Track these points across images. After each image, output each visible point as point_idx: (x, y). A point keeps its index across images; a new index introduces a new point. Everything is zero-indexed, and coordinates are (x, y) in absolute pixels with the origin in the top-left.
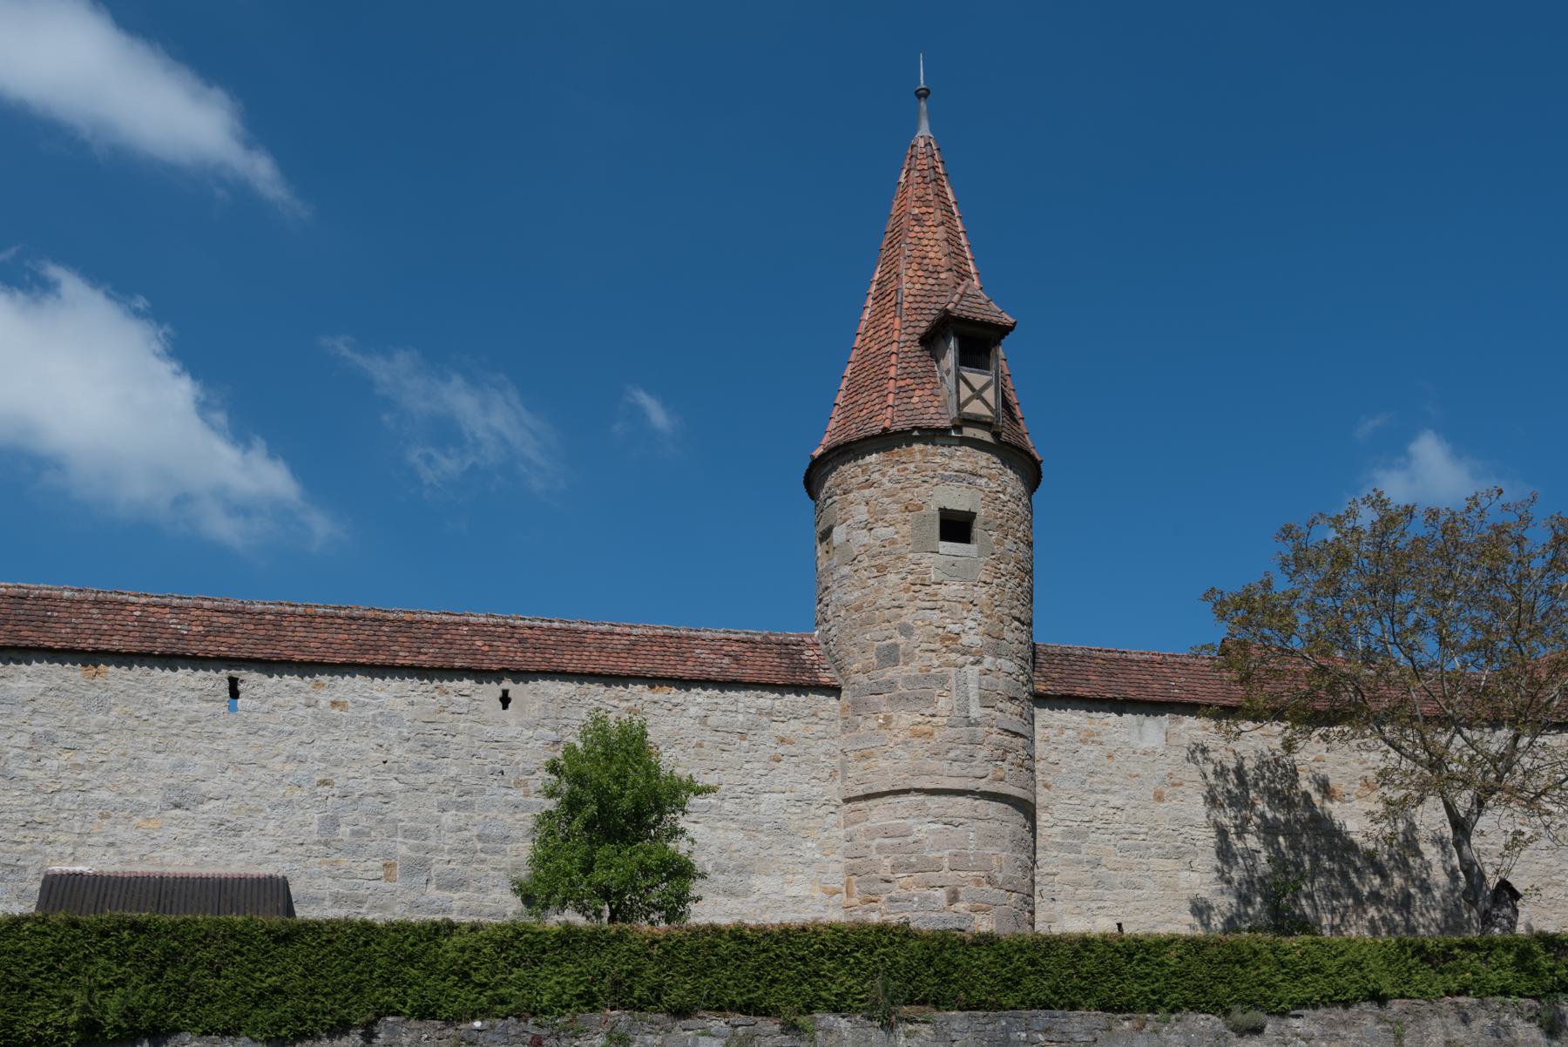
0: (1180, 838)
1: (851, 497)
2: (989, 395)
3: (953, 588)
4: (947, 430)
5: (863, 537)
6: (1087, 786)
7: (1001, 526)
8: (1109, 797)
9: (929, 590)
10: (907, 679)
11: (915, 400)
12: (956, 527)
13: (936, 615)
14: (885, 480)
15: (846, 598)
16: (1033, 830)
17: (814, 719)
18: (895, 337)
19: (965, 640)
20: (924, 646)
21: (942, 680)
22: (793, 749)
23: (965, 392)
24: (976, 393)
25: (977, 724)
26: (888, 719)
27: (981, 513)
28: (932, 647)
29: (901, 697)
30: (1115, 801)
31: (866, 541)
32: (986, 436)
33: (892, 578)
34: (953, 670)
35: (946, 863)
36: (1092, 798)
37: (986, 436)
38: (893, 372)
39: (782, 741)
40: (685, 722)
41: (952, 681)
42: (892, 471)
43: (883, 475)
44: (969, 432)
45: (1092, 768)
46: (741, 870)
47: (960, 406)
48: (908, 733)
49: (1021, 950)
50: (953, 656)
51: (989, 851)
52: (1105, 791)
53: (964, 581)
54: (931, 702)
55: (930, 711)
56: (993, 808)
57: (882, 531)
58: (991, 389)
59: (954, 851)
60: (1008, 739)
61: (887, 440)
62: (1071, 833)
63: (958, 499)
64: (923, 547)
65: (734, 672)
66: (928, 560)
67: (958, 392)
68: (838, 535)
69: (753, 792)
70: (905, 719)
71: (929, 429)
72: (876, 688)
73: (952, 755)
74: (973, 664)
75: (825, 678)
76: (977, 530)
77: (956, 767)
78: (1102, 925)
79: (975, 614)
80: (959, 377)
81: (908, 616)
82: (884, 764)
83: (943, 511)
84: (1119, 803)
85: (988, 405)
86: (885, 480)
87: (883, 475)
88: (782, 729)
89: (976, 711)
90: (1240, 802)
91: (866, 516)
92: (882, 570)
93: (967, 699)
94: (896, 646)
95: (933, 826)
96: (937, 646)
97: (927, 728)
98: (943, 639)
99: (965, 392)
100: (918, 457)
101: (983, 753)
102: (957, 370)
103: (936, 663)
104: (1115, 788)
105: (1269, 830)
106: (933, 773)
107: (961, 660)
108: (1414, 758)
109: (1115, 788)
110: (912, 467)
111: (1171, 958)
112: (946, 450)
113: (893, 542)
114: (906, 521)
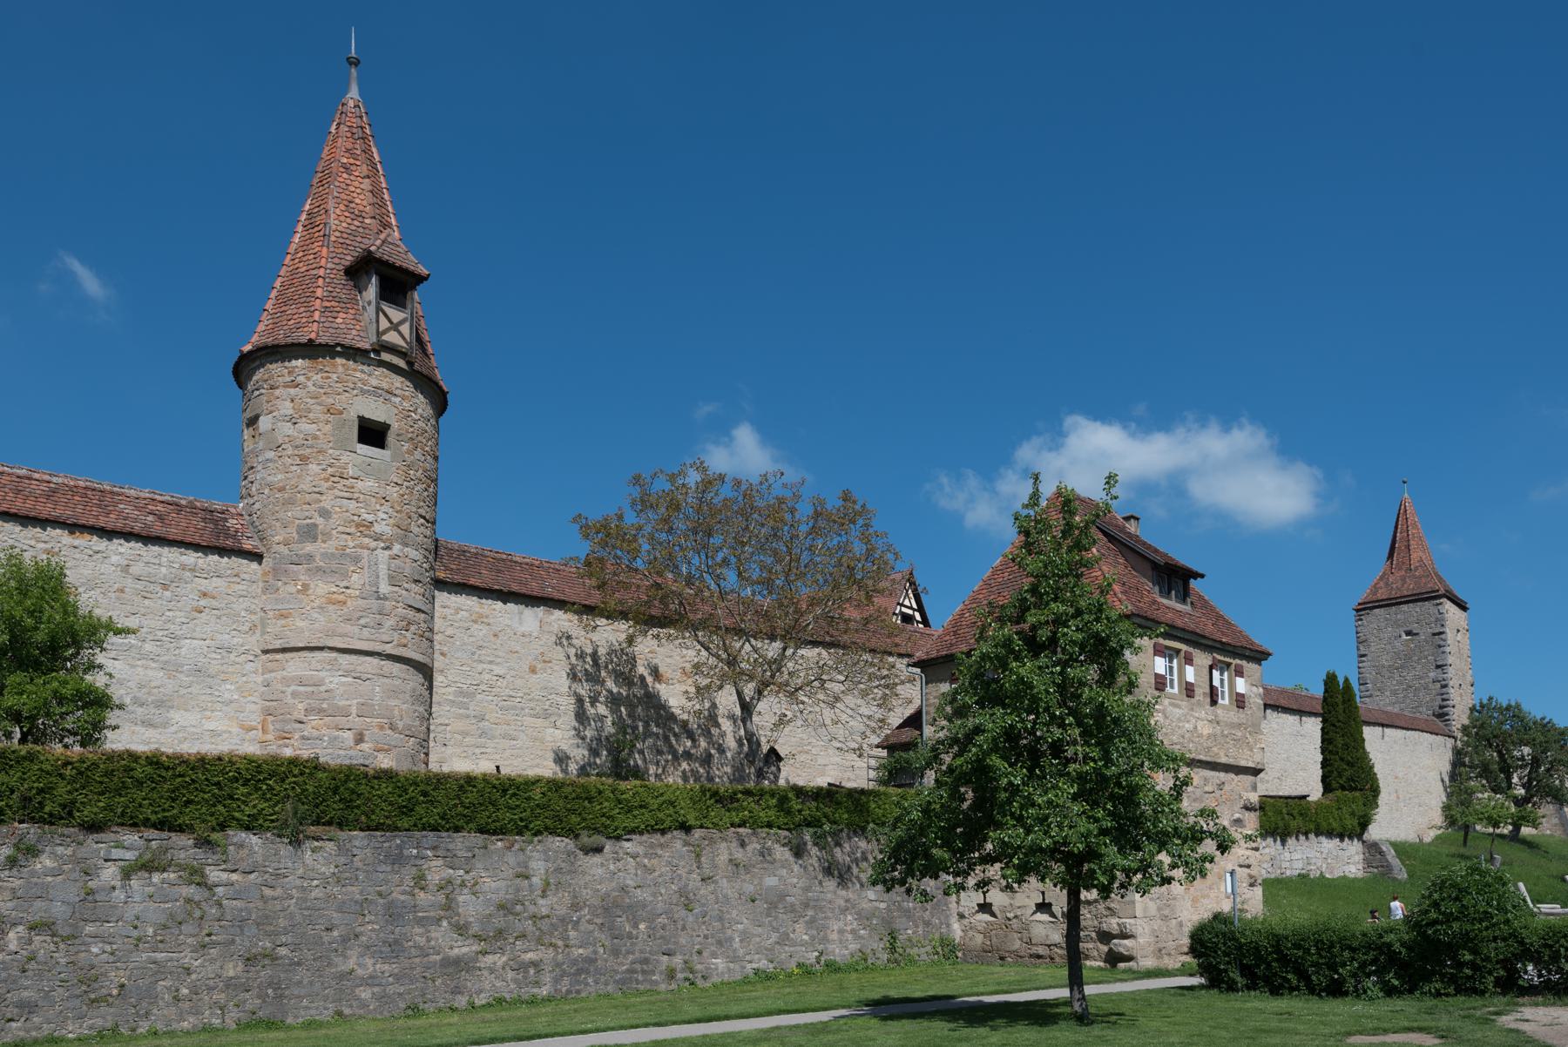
1: (277, 392)
2: (405, 329)
3: (369, 484)
5: (287, 428)
10: (324, 555)
11: (339, 320)
12: (372, 434)
13: (352, 505)
14: (310, 384)
15: (270, 479)
16: (430, 688)
18: (323, 262)
21: (356, 560)
22: (214, 603)
23: (384, 324)
24: (396, 326)
26: (306, 587)
29: (319, 569)
31: (290, 432)
32: (402, 364)
33: (314, 468)
35: (354, 710)
37: (402, 364)
38: (319, 293)
39: (205, 595)
41: (365, 562)
42: (317, 377)
43: (308, 379)
44: (386, 357)
46: (160, 704)
47: (379, 334)
49: (415, 784)
50: (366, 540)
53: (378, 479)
54: (346, 576)
55: (345, 583)
56: (397, 668)
57: (304, 426)
58: (407, 325)
60: (411, 614)
61: (312, 350)
62: (461, 693)
63: (377, 411)
64: (342, 445)
65: (158, 530)
66: (346, 457)
68: (264, 423)
69: (174, 637)
70: (321, 588)
71: (351, 348)
72: (295, 559)
73: (362, 621)
75: (248, 545)
76: (391, 438)
77: (366, 632)
79: (386, 507)
80: (379, 309)
81: (327, 503)
82: (300, 624)
83: (361, 419)
86: (310, 384)
87: (308, 379)
88: (203, 584)
90: (593, 678)
91: (291, 412)
92: (304, 459)
94: (315, 525)
96: (352, 530)
97: (341, 597)
98: (358, 526)
99: (384, 324)
100: (340, 369)
101: (389, 623)
102: (378, 304)
103: (351, 544)
105: (614, 701)
106: (346, 635)
107: (373, 544)
108: (718, 657)
110: (334, 376)
111: (536, 794)
112: (365, 368)
113: (316, 437)
114: (327, 422)
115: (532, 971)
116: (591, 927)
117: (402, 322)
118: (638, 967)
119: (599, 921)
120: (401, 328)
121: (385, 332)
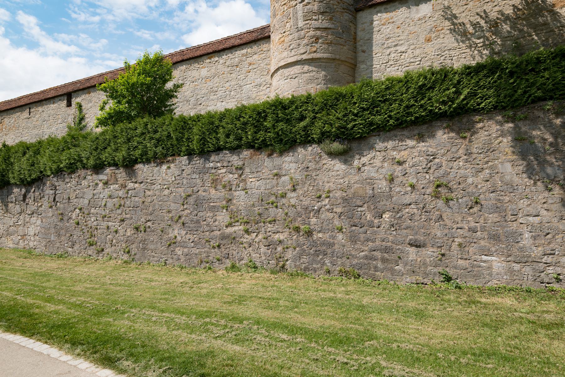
0: (442, 58)
6: (385, 46)
8: (398, 48)
17: (262, 52)
20: (282, 3)
22: (254, 66)
25: (302, 30)
28: (284, 2)
30: (401, 49)
34: (292, 9)
36: (388, 51)
40: (220, 66)
41: (291, 15)
45: (387, 37)
48: (278, 44)
51: (310, 86)
73: (291, 47)
74: (300, 3)
77: (293, 53)
78: (231, 105)
84: (403, 50)
88: (250, 60)
89: (301, 24)
93: (297, 19)
95: (286, 81)
103: (286, 9)
104: (401, 42)
109: (401, 42)
115: (279, 249)
116: (331, 215)
118: (378, 254)
119: (339, 210)
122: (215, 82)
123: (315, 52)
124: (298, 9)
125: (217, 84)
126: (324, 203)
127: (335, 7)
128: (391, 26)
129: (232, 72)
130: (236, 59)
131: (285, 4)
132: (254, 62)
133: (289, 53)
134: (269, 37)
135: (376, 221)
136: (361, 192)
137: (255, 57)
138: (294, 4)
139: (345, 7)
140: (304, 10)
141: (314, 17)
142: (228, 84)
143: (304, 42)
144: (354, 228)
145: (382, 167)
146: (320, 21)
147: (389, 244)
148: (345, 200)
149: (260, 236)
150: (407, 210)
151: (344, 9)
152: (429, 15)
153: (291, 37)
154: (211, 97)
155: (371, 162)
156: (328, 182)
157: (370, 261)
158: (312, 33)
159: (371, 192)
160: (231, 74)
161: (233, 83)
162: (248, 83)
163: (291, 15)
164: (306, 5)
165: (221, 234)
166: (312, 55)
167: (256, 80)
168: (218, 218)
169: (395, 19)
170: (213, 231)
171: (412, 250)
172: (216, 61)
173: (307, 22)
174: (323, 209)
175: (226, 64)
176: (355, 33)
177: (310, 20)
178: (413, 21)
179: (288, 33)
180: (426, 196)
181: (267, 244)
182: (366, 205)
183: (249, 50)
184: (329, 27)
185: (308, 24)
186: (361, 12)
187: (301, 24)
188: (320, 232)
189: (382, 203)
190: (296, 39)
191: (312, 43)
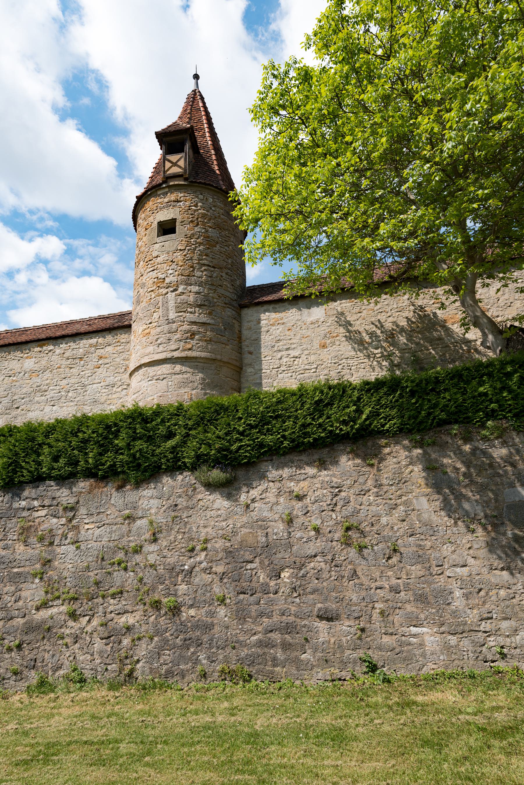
0: (340, 367)
2: (182, 163)
4: (160, 184)
6: (276, 348)
7: (192, 221)
8: (290, 352)
9: (152, 262)
12: (167, 228)
17: (119, 344)
19: (167, 280)
20: (149, 290)
22: (107, 361)
25: (174, 322)
27: (179, 218)
28: (152, 289)
30: (293, 353)
34: (161, 297)
36: (279, 355)
40: (54, 358)
41: (160, 304)
45: (278, 338)
47: (165, 172)
48: (141, 336)
51: (182, 391)
52: (288, 349)
55: (150, 321)
58: (183, 160)
59: (160, 394)
67: (164, 166)
73: (159, 342)
74: (172, 292)
77: (161, 348)
79: (174, 266)
84: (296, 354)
85: (180, 167)
88: (100, 352)
89: (172, 315)
93: (168, 310)
95: (150, 382)
103: (153, 296)
104: (293, 346)
107: (164, 291)
109: (293, 346)
115: (126, 641)
116: (208, 578)
117: (178, 161)
118: (276, 637)
119: (220, 569)
120: (178, 163)
121: (168, 170)
122: (46, 377)
123: (190, 349)
124: (169, 298)
125: (48, 381)
126: (198, 559)
127: (215, 300)
128: (281, 327)
129: (73, 366)
130: (81, 350)
131: (152, 291)
132: (107, 355)
133: (156, 348)
134: (129, 326)
135: (272, 583)
136: (251, 540)
137: (109, 349)
138: (164, 292)
139: (227, 302)
140: (176, 300)
141: (189, 310)
142: (65, 382)
143: (176, 337)
144: (242, 596)
145: (277, 503)
146: (197, 314)
147: (292, 619)
148: (229, 553)
149: (95, 622)
150: (312, 565)
151: (226, 304)
152: (322, 319)
153: (158, 330)
154: (36, 399)
155: (263, 496)
156: (205, 527)
157: (266, 650)
158: (186, 327)
159: (264, 539)
160: (71, 368)
161: (73, 381)
162: (96, 381)
163: (160, 304)
164: (180, 295)
165: (26, 623)
166: (186, 352)
167: (108, 379)
168: (23, 594)
169: (285, 321)
170: (12, 618)
171: (322, 625)
172: (50, 351)
173: (180, 314)
174: (197, 569)
175: (65, 355)
176: (240, 331)
177: (184, 312)
178: (305, 324)
179: (156, 324)
180: (334, 543)
181: (106, 635)
182: (257, 560)
183: (100, 339)
184: (208, 322)
185: (181, 316)
186: (246, 309)
187: (172, 315)
188: (191, 606)
189: (279, 556)
190: (165, 332)
191: (187, 339)
